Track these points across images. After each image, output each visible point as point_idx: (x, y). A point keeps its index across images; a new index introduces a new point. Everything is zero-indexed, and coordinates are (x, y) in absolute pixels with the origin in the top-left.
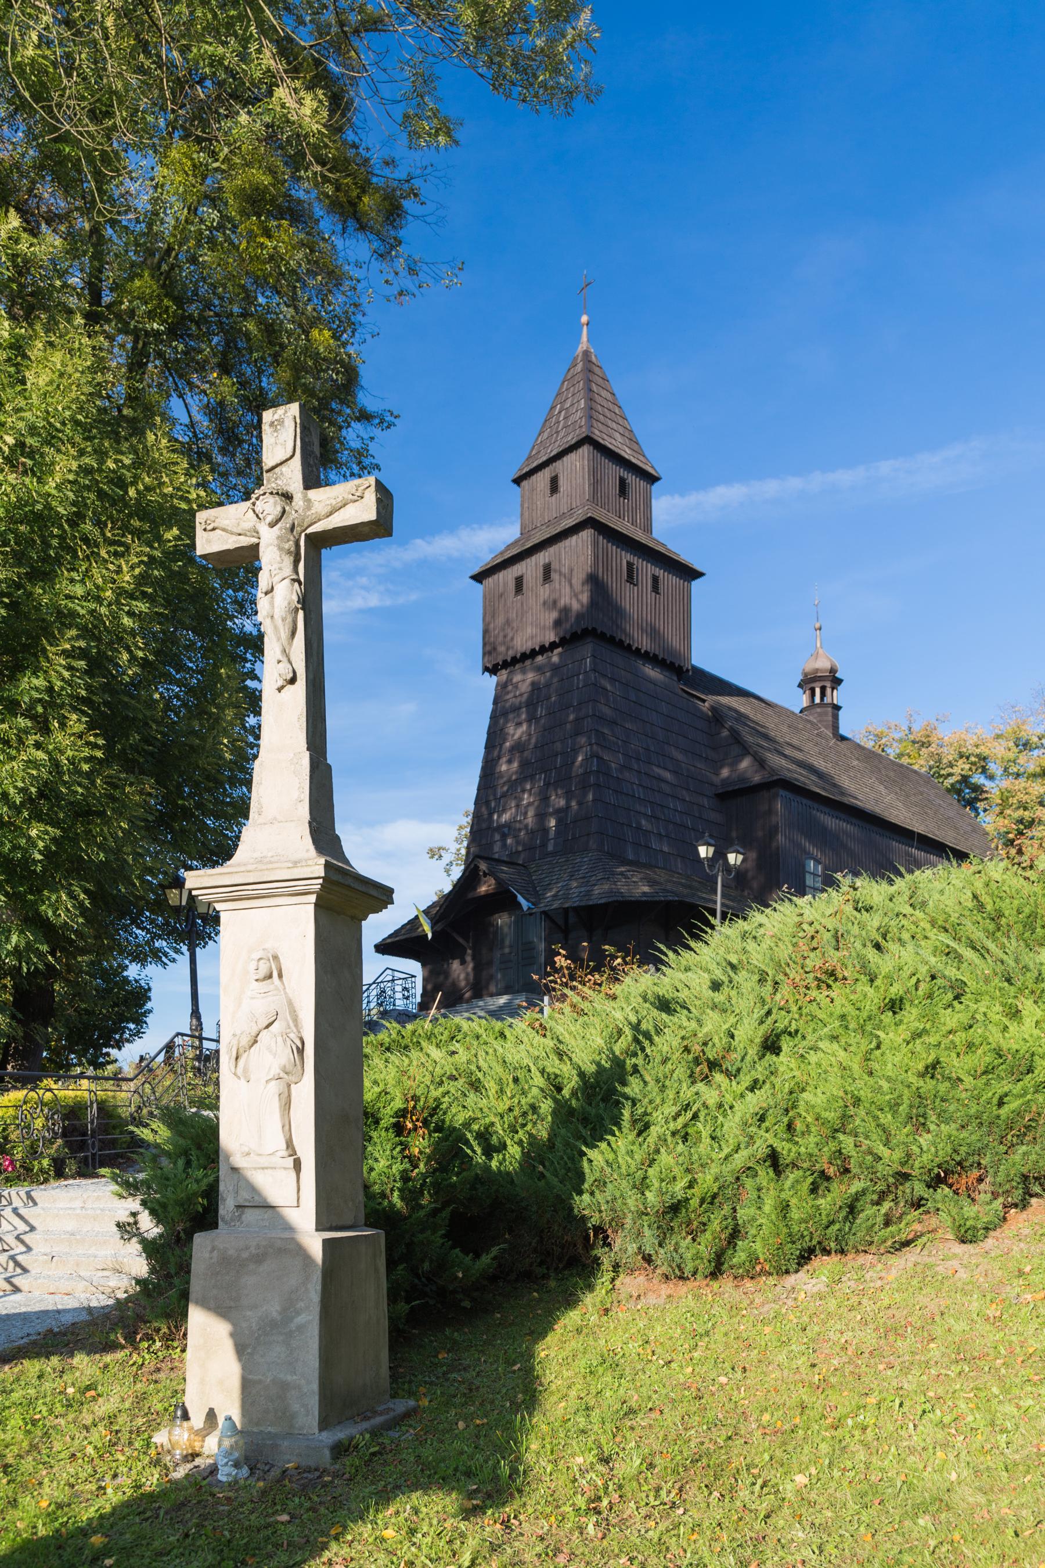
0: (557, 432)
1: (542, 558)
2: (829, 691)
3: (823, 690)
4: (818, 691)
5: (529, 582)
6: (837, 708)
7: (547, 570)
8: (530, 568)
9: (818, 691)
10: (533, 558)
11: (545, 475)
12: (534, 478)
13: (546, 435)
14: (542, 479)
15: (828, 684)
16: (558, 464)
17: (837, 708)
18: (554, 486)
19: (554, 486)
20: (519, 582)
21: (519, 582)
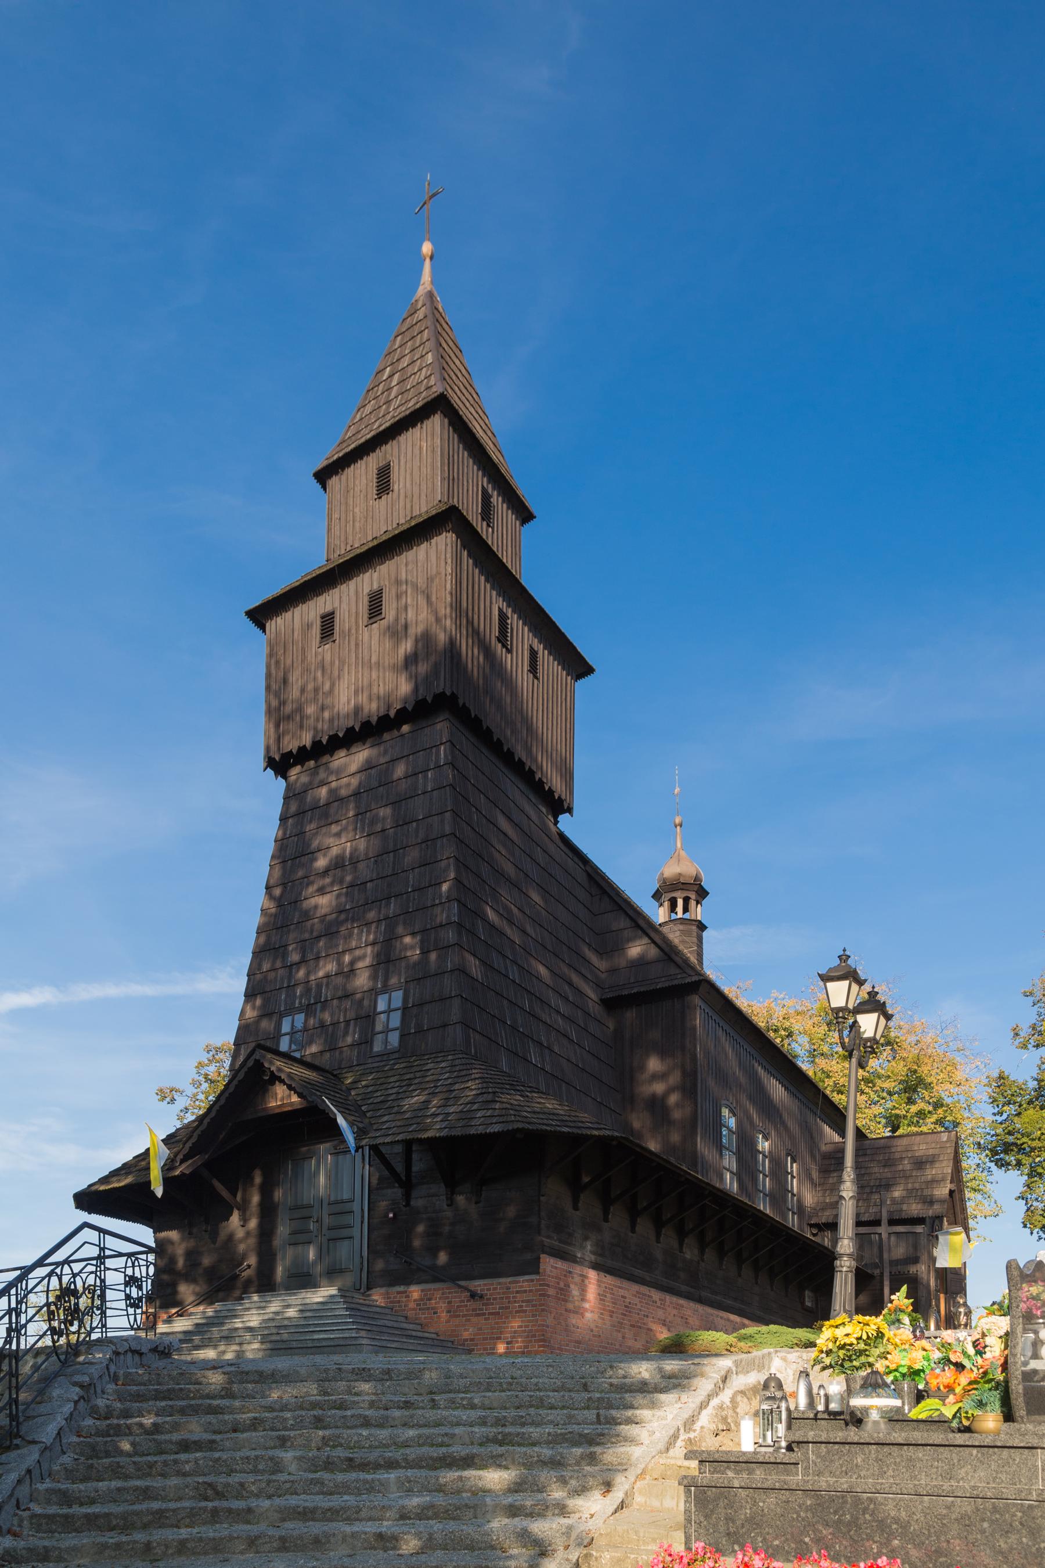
0: (388, 402)
1: (366, 582)
2: (693, 903)
3: (686, 900)
4: (680, 903)
5: (343, 622)
6: (702, 927)
7: (375, 606)
8: (347, 600)
9: (680, 903)
10: (352, 584)
11: (370, 464)
12: (350, 471)
13: (368, 409)
14: (362, 475)
15: (693, 896)
16: (388, 451)
17: (702, 927)
18: (384, 483)
19: (384, 483)
20: (328, 622)
21: (328, 622)
